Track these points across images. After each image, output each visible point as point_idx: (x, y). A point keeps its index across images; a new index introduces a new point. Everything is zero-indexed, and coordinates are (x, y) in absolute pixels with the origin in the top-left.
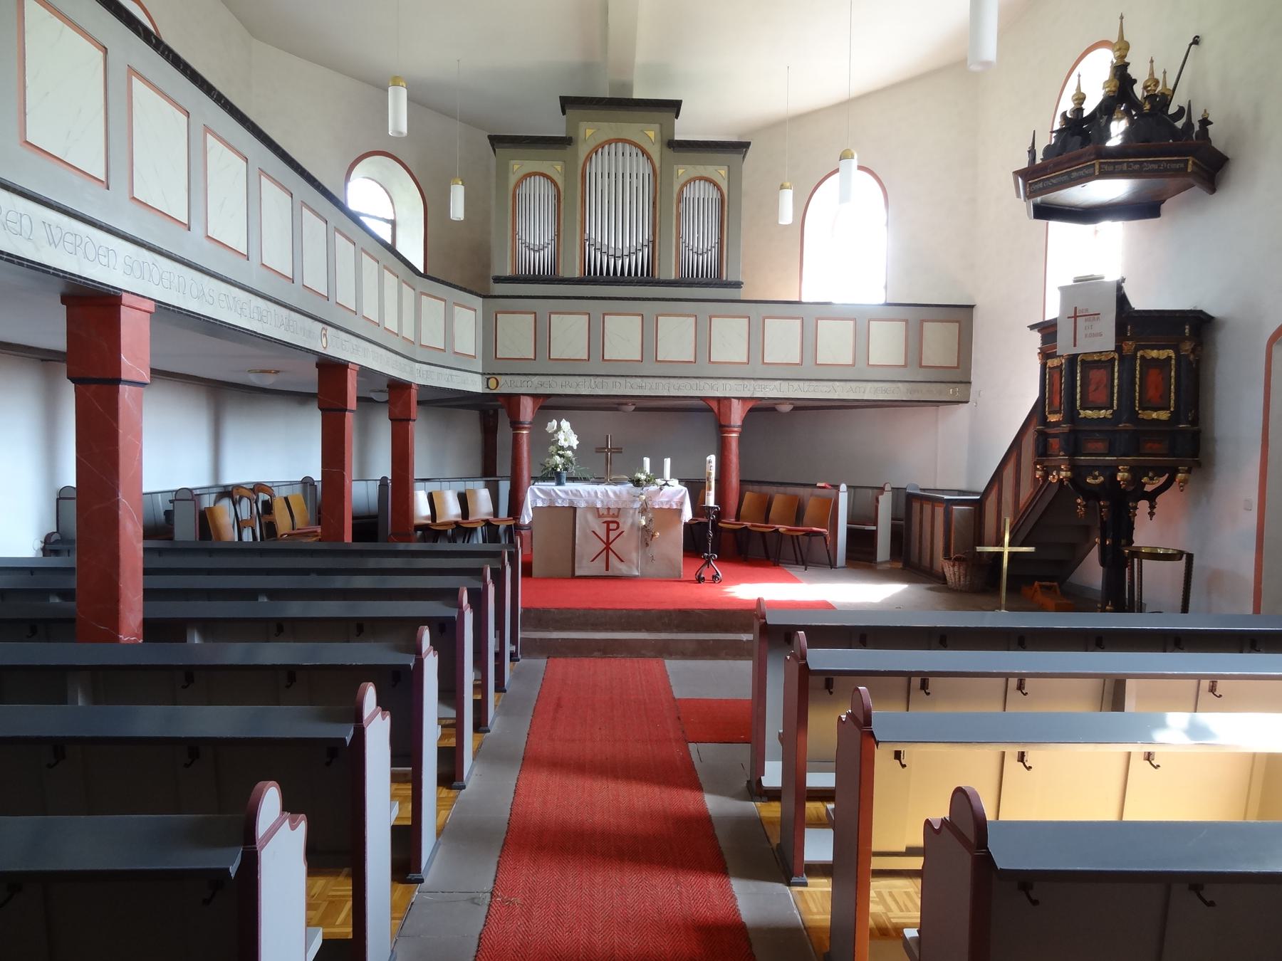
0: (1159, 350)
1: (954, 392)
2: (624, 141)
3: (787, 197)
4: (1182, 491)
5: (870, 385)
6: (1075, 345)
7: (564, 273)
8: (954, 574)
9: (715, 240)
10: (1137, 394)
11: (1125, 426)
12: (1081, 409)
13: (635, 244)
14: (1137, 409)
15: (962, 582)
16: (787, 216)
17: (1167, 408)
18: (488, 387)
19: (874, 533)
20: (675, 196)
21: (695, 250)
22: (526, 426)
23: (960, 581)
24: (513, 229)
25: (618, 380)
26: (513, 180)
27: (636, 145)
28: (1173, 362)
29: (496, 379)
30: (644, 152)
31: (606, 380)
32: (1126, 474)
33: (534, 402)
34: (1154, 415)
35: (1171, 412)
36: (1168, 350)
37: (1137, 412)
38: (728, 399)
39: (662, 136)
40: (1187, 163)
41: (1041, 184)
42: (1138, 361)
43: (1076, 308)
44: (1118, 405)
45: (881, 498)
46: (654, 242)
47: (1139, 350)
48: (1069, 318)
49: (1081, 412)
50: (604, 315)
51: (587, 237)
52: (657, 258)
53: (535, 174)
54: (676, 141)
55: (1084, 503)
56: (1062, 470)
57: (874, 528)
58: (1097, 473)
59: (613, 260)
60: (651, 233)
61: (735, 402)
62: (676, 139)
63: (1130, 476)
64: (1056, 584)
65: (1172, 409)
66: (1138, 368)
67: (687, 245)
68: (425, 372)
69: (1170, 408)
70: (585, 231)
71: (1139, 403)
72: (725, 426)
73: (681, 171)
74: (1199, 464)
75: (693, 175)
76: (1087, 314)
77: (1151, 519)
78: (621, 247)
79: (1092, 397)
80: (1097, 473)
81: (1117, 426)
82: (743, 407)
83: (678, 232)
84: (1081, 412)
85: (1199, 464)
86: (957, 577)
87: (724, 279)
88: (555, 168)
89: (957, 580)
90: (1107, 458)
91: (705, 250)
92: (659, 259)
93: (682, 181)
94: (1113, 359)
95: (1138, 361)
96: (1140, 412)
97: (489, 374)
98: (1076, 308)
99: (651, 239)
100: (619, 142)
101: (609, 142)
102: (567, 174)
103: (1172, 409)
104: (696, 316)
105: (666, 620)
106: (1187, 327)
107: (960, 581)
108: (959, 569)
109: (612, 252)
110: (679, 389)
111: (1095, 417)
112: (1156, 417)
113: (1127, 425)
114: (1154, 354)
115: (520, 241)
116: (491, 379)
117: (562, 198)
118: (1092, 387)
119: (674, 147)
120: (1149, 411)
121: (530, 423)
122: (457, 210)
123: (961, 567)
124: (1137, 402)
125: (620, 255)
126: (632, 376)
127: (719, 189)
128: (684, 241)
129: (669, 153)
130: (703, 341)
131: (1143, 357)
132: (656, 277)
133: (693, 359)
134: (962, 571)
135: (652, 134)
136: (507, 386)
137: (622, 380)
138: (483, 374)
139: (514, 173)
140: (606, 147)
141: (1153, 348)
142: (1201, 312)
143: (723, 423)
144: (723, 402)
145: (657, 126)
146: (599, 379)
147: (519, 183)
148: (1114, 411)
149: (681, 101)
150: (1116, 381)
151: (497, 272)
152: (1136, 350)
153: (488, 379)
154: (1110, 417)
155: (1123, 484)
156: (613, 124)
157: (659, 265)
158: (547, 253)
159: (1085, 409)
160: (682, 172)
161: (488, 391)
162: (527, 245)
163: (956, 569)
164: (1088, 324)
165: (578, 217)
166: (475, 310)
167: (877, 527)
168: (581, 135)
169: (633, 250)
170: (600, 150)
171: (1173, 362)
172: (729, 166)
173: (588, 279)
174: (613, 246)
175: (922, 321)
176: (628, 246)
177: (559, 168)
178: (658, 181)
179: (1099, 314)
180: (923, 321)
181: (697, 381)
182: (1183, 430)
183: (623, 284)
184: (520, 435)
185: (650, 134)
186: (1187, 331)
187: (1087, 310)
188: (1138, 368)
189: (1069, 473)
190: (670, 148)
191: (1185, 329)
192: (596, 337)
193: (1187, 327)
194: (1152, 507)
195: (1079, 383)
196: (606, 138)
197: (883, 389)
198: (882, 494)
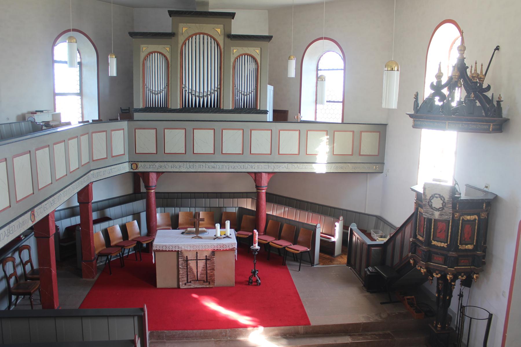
1: (376, 168)
2: (204, 34)
3: (292, 65)
7: (171, 106)
9: (253, 87)
10: (459, 238)
12: (433, 240)
13: (210, 90)
14: (458, 244)
16: (292, 73)
18: (132, 168)
20: (232, 64)
21: (243, 93)
22: (153, 188)
24: (143, 83)
25: (201, 164)
26: (143, 55)
27: (211, 37)
28: (477, 221)
29: (135, 164)
30: (214, 40)
31: (195, 164)
33: (157, 175)
35: (474, 246)
36: (475, 216)
37: (458, 246)
38: (261, 173)
39: (224, 33)
40: (490, 126)
41: (420, 122)
46: (220, 89)
49: (433, 241)
50: (194, 129)
51: (184, 86)
52: (222, 98)
53: (155, 52)
54: (232, 35)
59: (198, 99)
60: (219, 84)
61: (264, 174)
62: (232, 34)
63: (453, 277)
65: (475, 244)
67: (238, 90)
68: (96, 174)
69: (474, 243)
70: (182, 84)
71: (461, 231)
72: (258, 187)
73: (235, 51)
75: (241, 53)
78: (202, 92)
82: (268, 177)
83: (233, 83)
84: (433, 241)
87: (258, 109)
88: (166, 49)
90: (443, 266)
91: (248, 93)
92: (223, 98)
93: (236, 56)
97: (132, 162)
99: (219, 87)
100: (201, 34)
101: (195, 34)
102: (173, 52)
103: (475, 244)
104: (243, 129)
105: (224, 334)
106: (484, 205)
109: (197, 94)
110: (234, 167)
113: (453, 253)
114: (468, 217)
115: (147, 89)
116: (134, 164)
117: (170, 66)
118: (438, 231)
119: (231, 38)
121: (156, 186)
122: (113, 71)
124: (459, 241)
125: (202, 96)
126: (209, 162)
127: (256, 61)
128: (236, 88)
129: (228, 40)
130: (247, 143)
131: (463, 219)
132: (222, 108)
133: (241, 152)
135: (219, 30)
136: (142, 168)
137: (204, 164)
138: (129, 162)
139: (143, 52)
140: (194, 37)
143: (257, 185)
144: (257, 176)
145: (222, 26)
146: (191, 164)
147: (145, 59)
149: (235, 13)
150: (450, 230)
151: (135, 107)
152: (460, 216)
153: (132, 164)
154: (446, 247)
156: (197, 25)
157: (223, 102)
158: (163, 94)
160: (236, 51)
161: (132, 170)
162: (151, 91)
165: (179, 76)
166: (123, 129)
168: (180, 31)
169: (209, 93)
170: (191, 38)
171: (477, 221)
172: (261, 48)
173: (186, 109)
174: (198, 91)
175: (361, 132)
176: (206, 91)
177: (168, 49)
178: (222, 57)
180: (361, 132)
181: (244, 164)
183: (204, 112)
184: (150, 193)
185: (218, 30)
186: (484, 207)
189: (425, 270)
190: (229, 38)
191: (483, 206)
192: (189, 142)
193: (484, 205)
195: (433, 227)
196: (194, 32)
197: (341, 166)
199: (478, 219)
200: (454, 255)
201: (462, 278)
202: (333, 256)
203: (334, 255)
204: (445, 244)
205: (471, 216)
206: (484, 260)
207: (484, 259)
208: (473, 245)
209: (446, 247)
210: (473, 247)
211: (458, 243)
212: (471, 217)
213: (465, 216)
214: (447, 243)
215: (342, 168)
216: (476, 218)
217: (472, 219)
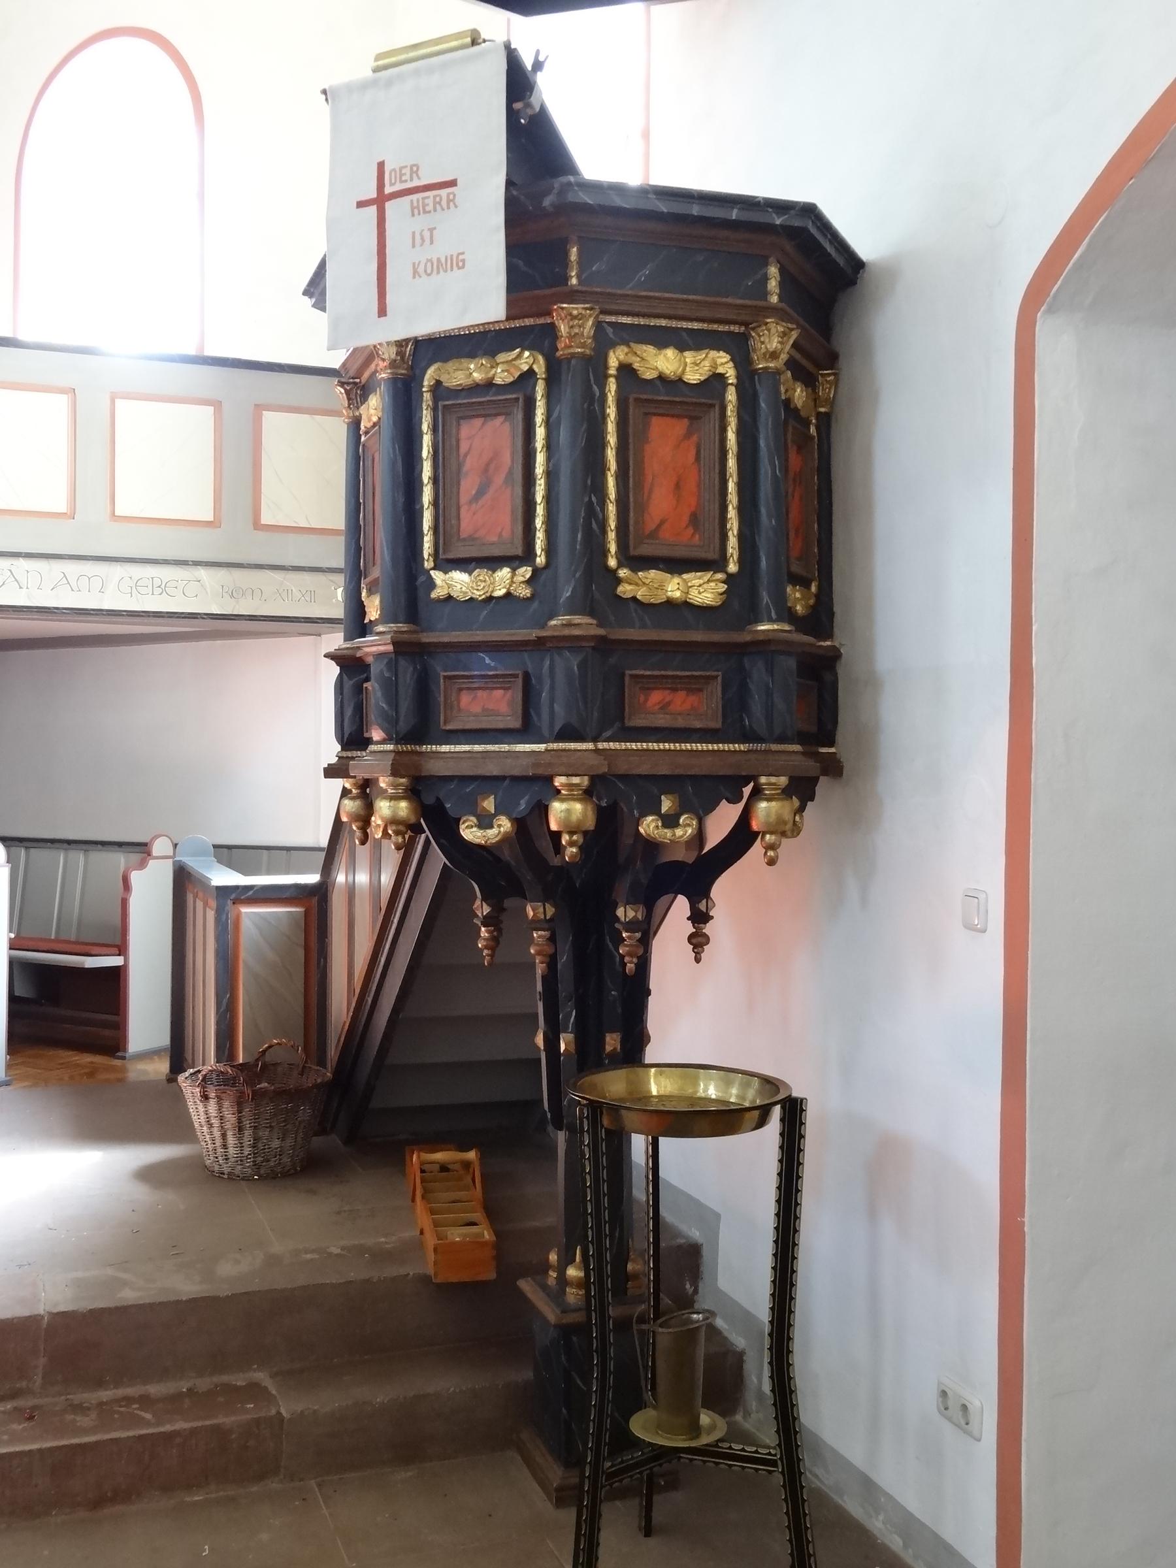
0: (682, 348)
4: (771, 862)
5: (118, 570)
6: (382, 312)
8: (211, 1126)
11: (569, 625)
12: (434, 569)
14: (612, 562)
15: (232, 1151)
17: (715, 564)
19: (115, 979)
23: (225, 1146)
28: (731, 395)
32: (578, 807)
34: (673, 587)
35: (730, 579)
37: (613, 572)
42: (612, 386)
43: (381, 166)
44: (550, 551)
45: (135, 877)
47: (613, 345)
48: (361, 204)
49: (437, 576)
55: (486, 910)
56: (383, 793)
57: (116, 961)
58: (489, 804)
64: (472, 1155)
65: (733, 568)
66: (612, 411)
74: (833, 768)
76: (416, 183)
77: (698, 960)
79: (469, 520)
80: (489, 804)
81: (543, 626)
84: (437, 576)
85: (833, 768)
86: (217, 1134)
89: (219, 1142)
94: (531, 373)
95: (612, 386)
96: (623, 573)
98: (381, 166)
103: (733, 568)
107: (225, 1146)
108: (220, 1110)
111: (479, 595)
112: (678, 594)
118: (468, 486)
120: (653, 573)
123: (226, 1104)
124: (612, 536)
134: (231, 1118)
141: (661, 339)
142: (810, 211)
148: (536, 572)
154: (525, 592)
155: (572, 844)
159: (446, 564)
163: (212, 1106)
164: (420, 223)
167: (126, 960)
171: (731, 395)
175: (259, 408)
179: (452, 183)
182: (764, 646)
186: (773, 284)
187: (415, 170)
188: (612, 411)
189: (403, 804)
191: (766, 279)
193: (773, 270)
194: (699, 918)
197: (157, 582)
198: (142, 865)
199: (738, 377)
200: (576, 632)
201: (668, 833)
202: (118, 1054)
203: (125, 1049)
204: (522, 570)
205: (687, 354)
206: (832, 750)
207: (831, 743)
208: (720, 576)
209: (525, 592)
210: (723, 587)
211: (605, 553)
212: (689, 356)
213: (649, 350)
214: (528, 556)
215: (163, 589)
216: (720, 370)
217: (693, 377)
